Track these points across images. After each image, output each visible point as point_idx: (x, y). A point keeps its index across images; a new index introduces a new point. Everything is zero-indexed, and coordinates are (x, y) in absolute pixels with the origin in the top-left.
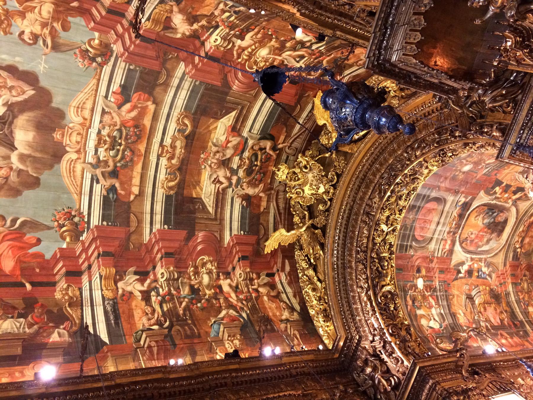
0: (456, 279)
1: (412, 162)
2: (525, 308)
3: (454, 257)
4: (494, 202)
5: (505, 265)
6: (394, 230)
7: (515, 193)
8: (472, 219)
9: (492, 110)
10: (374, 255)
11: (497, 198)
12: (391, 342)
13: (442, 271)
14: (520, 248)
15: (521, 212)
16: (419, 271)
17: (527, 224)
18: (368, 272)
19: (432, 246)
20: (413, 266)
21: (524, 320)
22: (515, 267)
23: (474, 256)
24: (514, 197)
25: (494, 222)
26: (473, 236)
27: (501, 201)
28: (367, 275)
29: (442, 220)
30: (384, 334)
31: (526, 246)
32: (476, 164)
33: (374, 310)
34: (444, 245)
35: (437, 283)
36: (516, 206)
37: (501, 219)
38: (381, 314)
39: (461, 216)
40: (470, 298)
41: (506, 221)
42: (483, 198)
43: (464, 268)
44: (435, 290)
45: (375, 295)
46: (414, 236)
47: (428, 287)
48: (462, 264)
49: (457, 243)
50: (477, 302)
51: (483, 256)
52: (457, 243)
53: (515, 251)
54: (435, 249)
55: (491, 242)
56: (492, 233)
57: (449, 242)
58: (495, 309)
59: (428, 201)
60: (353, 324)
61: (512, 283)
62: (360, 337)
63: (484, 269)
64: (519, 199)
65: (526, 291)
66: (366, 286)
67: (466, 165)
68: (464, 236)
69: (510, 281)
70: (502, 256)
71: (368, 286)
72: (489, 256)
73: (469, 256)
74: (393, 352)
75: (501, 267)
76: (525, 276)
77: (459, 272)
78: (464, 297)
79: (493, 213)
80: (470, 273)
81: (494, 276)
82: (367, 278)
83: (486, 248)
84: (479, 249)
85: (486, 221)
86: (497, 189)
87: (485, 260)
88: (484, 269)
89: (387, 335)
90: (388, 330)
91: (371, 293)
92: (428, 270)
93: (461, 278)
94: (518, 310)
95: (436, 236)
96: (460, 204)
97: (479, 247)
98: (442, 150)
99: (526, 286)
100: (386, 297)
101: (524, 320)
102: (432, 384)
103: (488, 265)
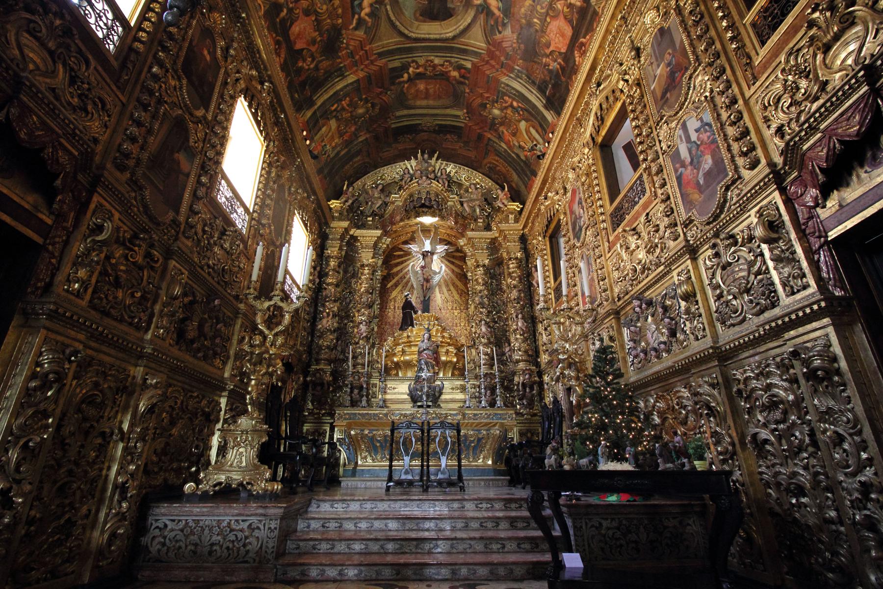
2: (332, 112)
5: (381, 55)
21: (316, 107)
53: (405, 68)
58: (313, 42)
61: (358, 81)
65: (354, 114)
76: (373, 105)
81: (360, 33)
94: (326, 97)
99: (361, 111)
101: (316, 107)
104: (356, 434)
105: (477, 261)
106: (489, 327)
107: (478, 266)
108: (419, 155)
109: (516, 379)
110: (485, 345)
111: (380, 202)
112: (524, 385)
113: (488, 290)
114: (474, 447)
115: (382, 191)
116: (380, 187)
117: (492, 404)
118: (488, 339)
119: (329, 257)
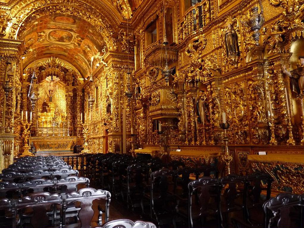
0: (38, 33)
1: (96, 17)
3: (47, 30)
4: (73, 38)
5: (43, 45)
6: (62, 12)
7: (77, 43)
8: (66, 33)
9: (121, 44)
10: (51, 7)
11: (75, 39)
12: (19, 26)
13: (41, 28)
14: (51, 47)
15: (69, 45)
16: (41, 21)
17: (63, 47)
18: (42, 7)
19: (52, 23)
20: (43, 19)
22: (43, 48)
23: (47, 35)
24: (76, 43)
25: (64, 39)
26: (57, 34)
27: (74, 39)
28: (41, 7)
29: (64, 24)
30: (21, 22)
31: (52, 49)
32: (93, 34)
33: (27, 14)
34: (53, 26)
35: (35, 28)
36: (71, 44)
37: (65, 40)
38: (27, 18)
39: (67, 29)
40: (30, 39)
41: (63, 41)
42: (75, 35)
43: (42, 34)
44: (33, 28)
45: (34, 13)
46: (57, 16)
47: (34, 26)
48: (44, 32)
49: (54, 30)
50: (28, 42)
51: (47, 38)
52: (54, 30)
54: (51, 24)
55: (54, 39)
56: (58, 39)
57: (54, 27)
59: (74, 20)
60: (13, 4)
62: (10, 10)
63: (42, 39)
64: (75, 44)
66: (37, 8)
67: (92, 31)
68: (57, 31)
69: (37, 48)
70: (48, 43)
71: (36, 9)
72: (48, 40)
73: (48, 34)
74: (16, 29)
75: (43, 44)
77: (40, 33)
78: (30, 37)
79: (68, 38)
80: (41, 36)
81: (39, 43)
82: (40, 7)
83: (51, 38)
84: (51, 36)
85: (64, 37)
86: (80, 39)
87: (46, 39)
88: (42, 39)
89: (21, 24)
90: (22, 24)
91: (34, 11)
92: (41, 24)
93: (38, 34)
95: (57, 23)
96: (73, 29)
97: (52, 36)
98: (104, 29)
100: (34, 17)
102: (17, 50)
103: (43, 40)
104: (36, 144)
105: (69, 95)
106: (71, 114)
107: (69, 96)
108: (52, 58)
109: (78, 129)
110: (70, 119)
111: (39, 74)
112: (79, 131)
113: (72, 104)
114: (66, 146)
115: (39, 69)
116: (38, 68)
117: (71, 135)
118: (71, 118)
119: (23, 93)
